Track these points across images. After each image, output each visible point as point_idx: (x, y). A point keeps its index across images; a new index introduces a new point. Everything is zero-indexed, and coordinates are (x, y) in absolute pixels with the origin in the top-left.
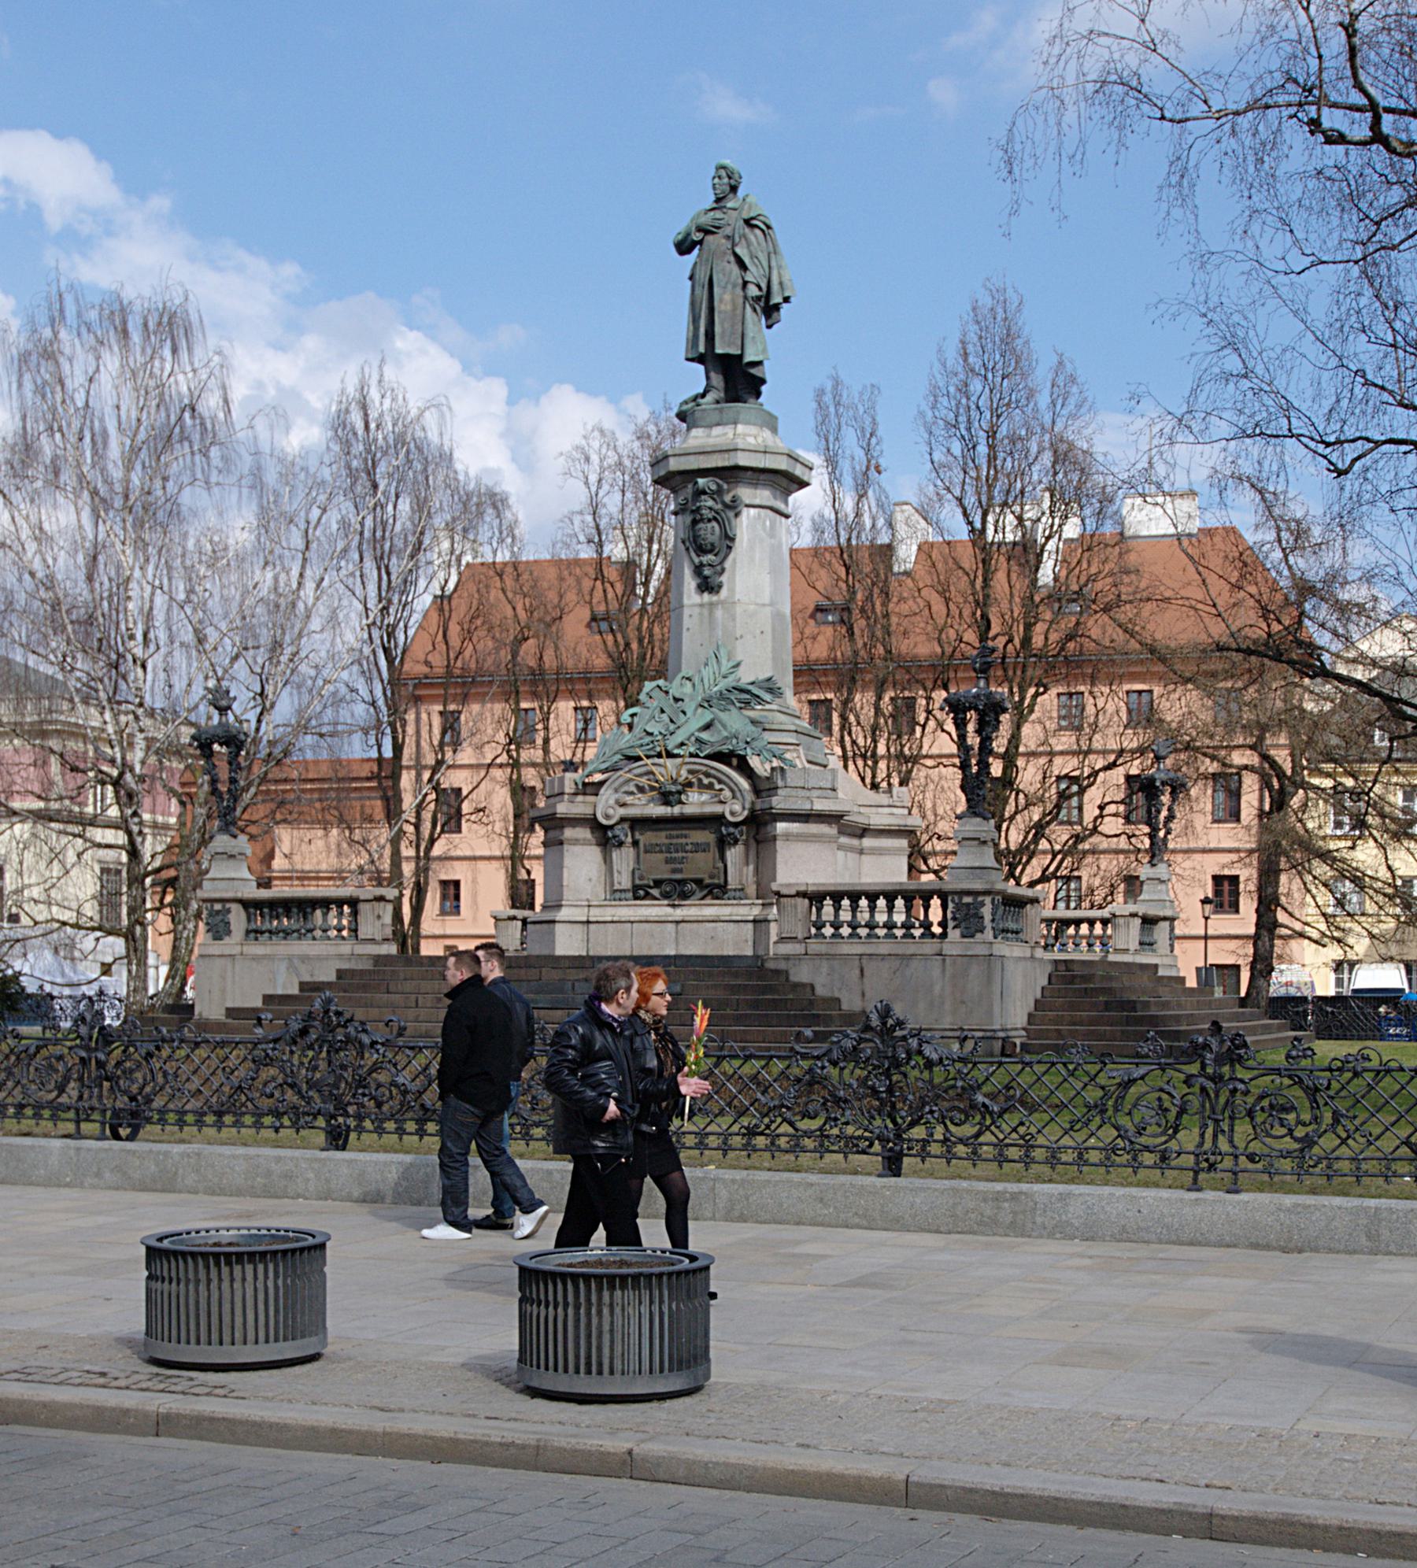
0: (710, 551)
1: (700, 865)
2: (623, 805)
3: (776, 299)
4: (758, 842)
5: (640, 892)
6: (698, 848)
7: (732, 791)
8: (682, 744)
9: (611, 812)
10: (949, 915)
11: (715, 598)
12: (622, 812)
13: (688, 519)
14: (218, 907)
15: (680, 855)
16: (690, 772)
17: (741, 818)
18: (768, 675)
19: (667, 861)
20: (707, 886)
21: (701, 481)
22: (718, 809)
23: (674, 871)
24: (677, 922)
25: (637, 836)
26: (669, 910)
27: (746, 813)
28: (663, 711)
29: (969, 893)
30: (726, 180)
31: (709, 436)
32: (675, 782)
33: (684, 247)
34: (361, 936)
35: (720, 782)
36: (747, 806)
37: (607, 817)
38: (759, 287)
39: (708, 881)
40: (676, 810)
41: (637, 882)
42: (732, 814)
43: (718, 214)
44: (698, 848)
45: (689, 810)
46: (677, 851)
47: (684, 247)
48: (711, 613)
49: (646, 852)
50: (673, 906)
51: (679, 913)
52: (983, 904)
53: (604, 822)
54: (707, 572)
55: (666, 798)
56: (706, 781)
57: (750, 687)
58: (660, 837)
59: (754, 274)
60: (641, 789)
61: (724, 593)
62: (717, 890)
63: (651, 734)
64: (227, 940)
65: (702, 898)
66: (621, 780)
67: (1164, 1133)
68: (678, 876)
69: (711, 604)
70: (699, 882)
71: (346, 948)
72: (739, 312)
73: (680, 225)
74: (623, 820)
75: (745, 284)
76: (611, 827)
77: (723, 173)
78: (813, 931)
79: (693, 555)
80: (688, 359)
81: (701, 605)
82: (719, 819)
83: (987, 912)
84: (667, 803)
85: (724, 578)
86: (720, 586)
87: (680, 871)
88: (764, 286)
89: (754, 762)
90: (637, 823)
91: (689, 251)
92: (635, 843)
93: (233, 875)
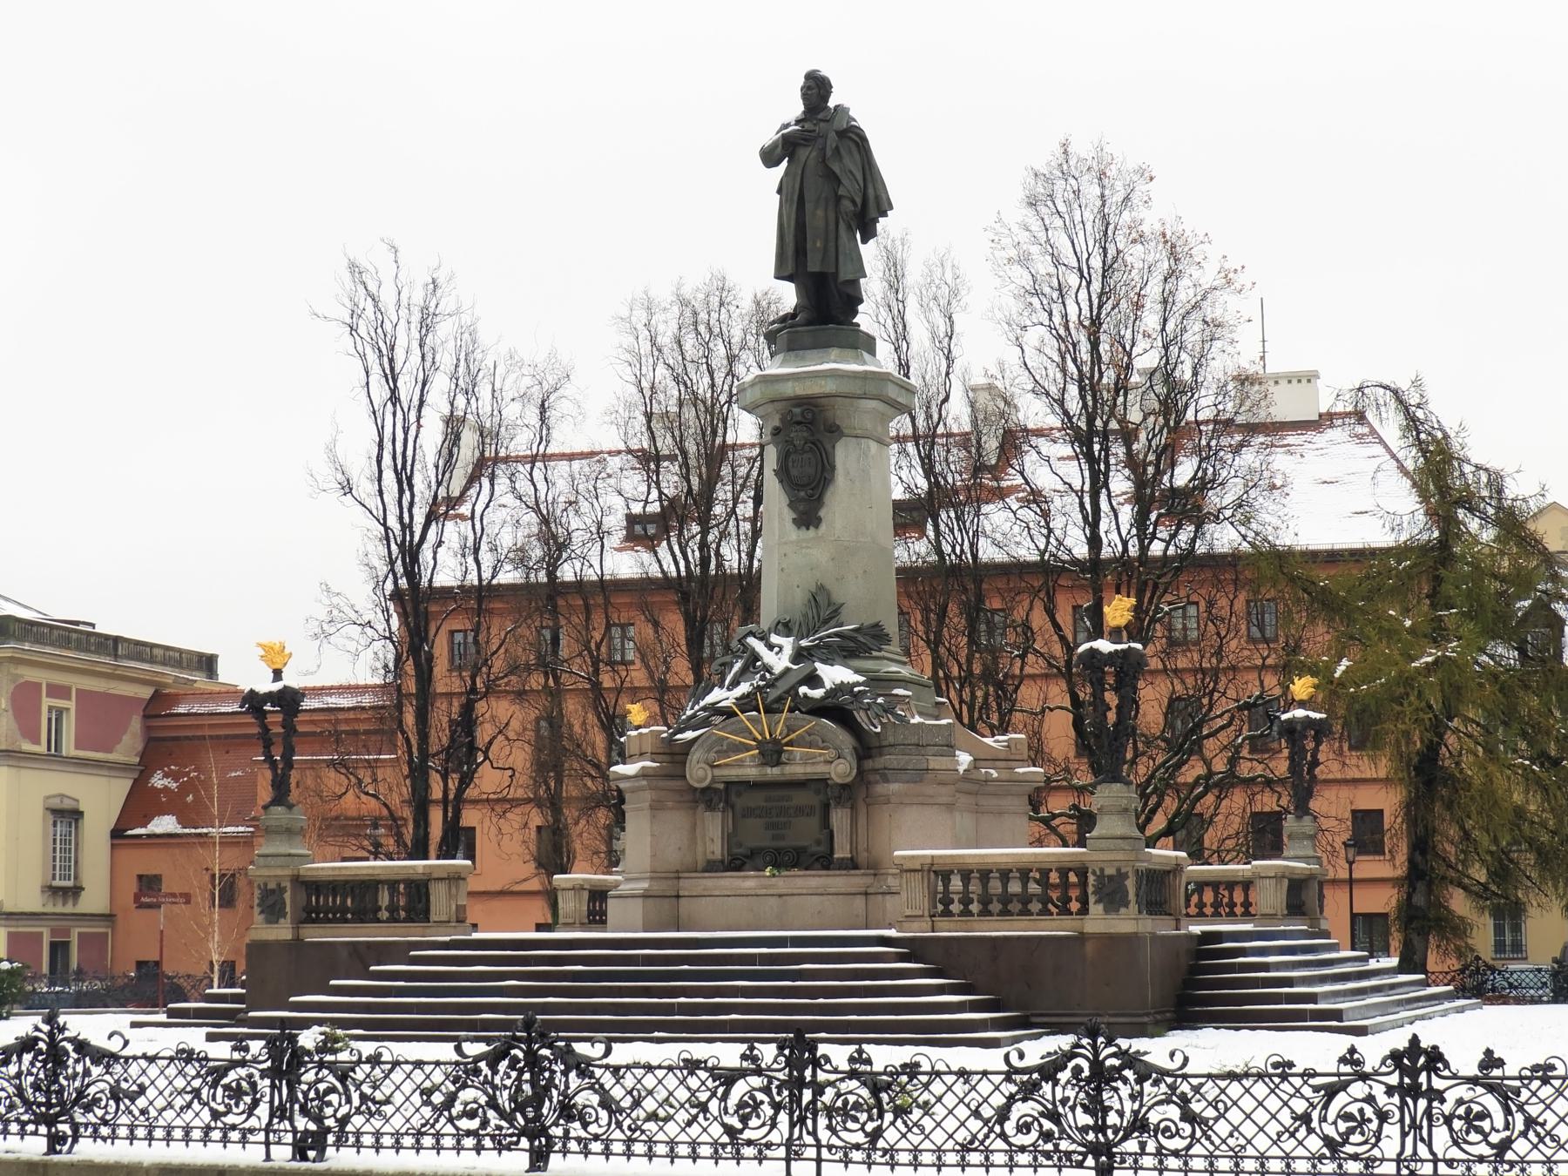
1: (804, 832)
3: (872, 213)
4: (868, 805)
5: (735, 862)
6: (800, 811)
8: (780, 699)
9: (701, 773)
10: (1090, 889)
11: (812, 532)
15: (782, 819)
16: (791, 730)
17: (849, 779)
18: (872, 621)
19: (769, 826)
22: (821, 769)
23: (774, 838)
33: (770, 157)
34: (433, 917)
38: (854, 202)
39: (815, 849)
41: (736, 851)
43: (808, 126)
44: (800, 811)
47: (770, 157)
52: (1126, 876)
56: (808, 738)
58: (756, 800)
59: (849, 187)
61: (823, 527)
62: (824, 861)
67: (1366, 1142)
68: (781, 844)
70: (800, 851)
72: (832, 227)
73: (769, 136)
74: (713, 780)
75: (838, 199)
77: (811, 83)
78: (940, 907)
80: (777, 277)
82: (822, 782)
83: (1130, 884)
86: (820, 520)
87: (782, 837)
88: (859, 201)
89: (860, 717)
90: (734, 787)
91: (777, 164)
92: (729, 805)
93: (293, 851)
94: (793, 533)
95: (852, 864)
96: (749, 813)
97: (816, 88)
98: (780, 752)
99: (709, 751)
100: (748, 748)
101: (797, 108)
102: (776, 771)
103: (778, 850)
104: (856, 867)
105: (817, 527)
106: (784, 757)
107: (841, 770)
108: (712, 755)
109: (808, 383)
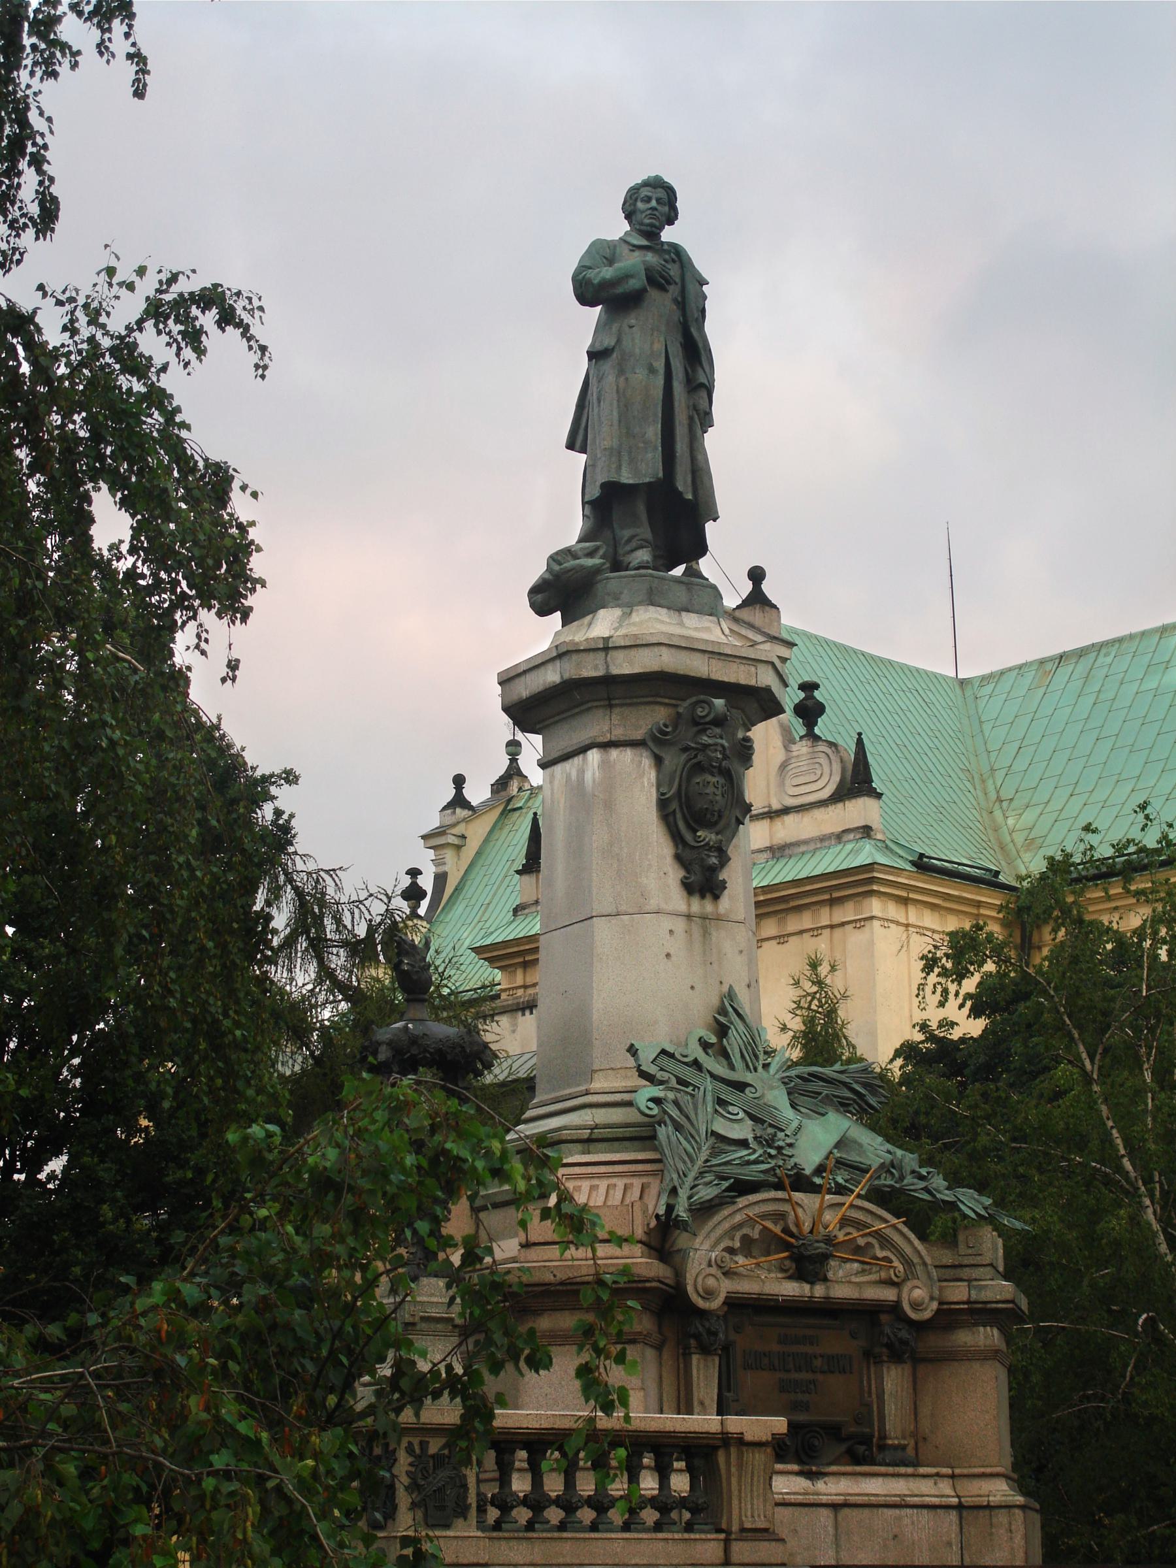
0: (710, 825)
6: (836, 1364)
8: (820, 1170)
9: (711, 1282)
11: (708, 906)
12: (726, 1286)
13: (674, 760)
16: (845, 1222)
17: (927, 1315)
20: (849, 1437)
21: (719, 702)
22: (889, 1294)
24: (835, 1507)
25: (733, 1336)
26: (802, 1483)
27: (935, 1305)
28: (721, 1102)
30: (666, 209)
31: (681, 624)
32: (829, 1240)
35: (885, 1242)
36: (936, 1293)
37: (709, 1294)
40: (819, 1291)
42: (916, 1306)
44: (836, 1364)
45: (841, 1292)
46: (799, 1369)
48: (706, 933)
49: (747, 1366)
50: (811, 1476)
51: (833, 1488)
53: (701, 1303)
55: (807, 1262)
56: (861, 1242)
57: (843, 1077)
62: (863, 1448)
63: (743, 1143)
66: (726, 1225)
69: (704, 918)
70: (834, 1431)
71: (709, 1549)
76: (702, 1313)
79: (681, 825)
81: (689, 917)
84: (800, 1275)
86: (723, 886)
97: (652, 205)
98: (825, 1257)
99: (713, 1248)
101: (617, 228)
102: (819, 1291)
105: (716, 897)
107: (919, 1297)
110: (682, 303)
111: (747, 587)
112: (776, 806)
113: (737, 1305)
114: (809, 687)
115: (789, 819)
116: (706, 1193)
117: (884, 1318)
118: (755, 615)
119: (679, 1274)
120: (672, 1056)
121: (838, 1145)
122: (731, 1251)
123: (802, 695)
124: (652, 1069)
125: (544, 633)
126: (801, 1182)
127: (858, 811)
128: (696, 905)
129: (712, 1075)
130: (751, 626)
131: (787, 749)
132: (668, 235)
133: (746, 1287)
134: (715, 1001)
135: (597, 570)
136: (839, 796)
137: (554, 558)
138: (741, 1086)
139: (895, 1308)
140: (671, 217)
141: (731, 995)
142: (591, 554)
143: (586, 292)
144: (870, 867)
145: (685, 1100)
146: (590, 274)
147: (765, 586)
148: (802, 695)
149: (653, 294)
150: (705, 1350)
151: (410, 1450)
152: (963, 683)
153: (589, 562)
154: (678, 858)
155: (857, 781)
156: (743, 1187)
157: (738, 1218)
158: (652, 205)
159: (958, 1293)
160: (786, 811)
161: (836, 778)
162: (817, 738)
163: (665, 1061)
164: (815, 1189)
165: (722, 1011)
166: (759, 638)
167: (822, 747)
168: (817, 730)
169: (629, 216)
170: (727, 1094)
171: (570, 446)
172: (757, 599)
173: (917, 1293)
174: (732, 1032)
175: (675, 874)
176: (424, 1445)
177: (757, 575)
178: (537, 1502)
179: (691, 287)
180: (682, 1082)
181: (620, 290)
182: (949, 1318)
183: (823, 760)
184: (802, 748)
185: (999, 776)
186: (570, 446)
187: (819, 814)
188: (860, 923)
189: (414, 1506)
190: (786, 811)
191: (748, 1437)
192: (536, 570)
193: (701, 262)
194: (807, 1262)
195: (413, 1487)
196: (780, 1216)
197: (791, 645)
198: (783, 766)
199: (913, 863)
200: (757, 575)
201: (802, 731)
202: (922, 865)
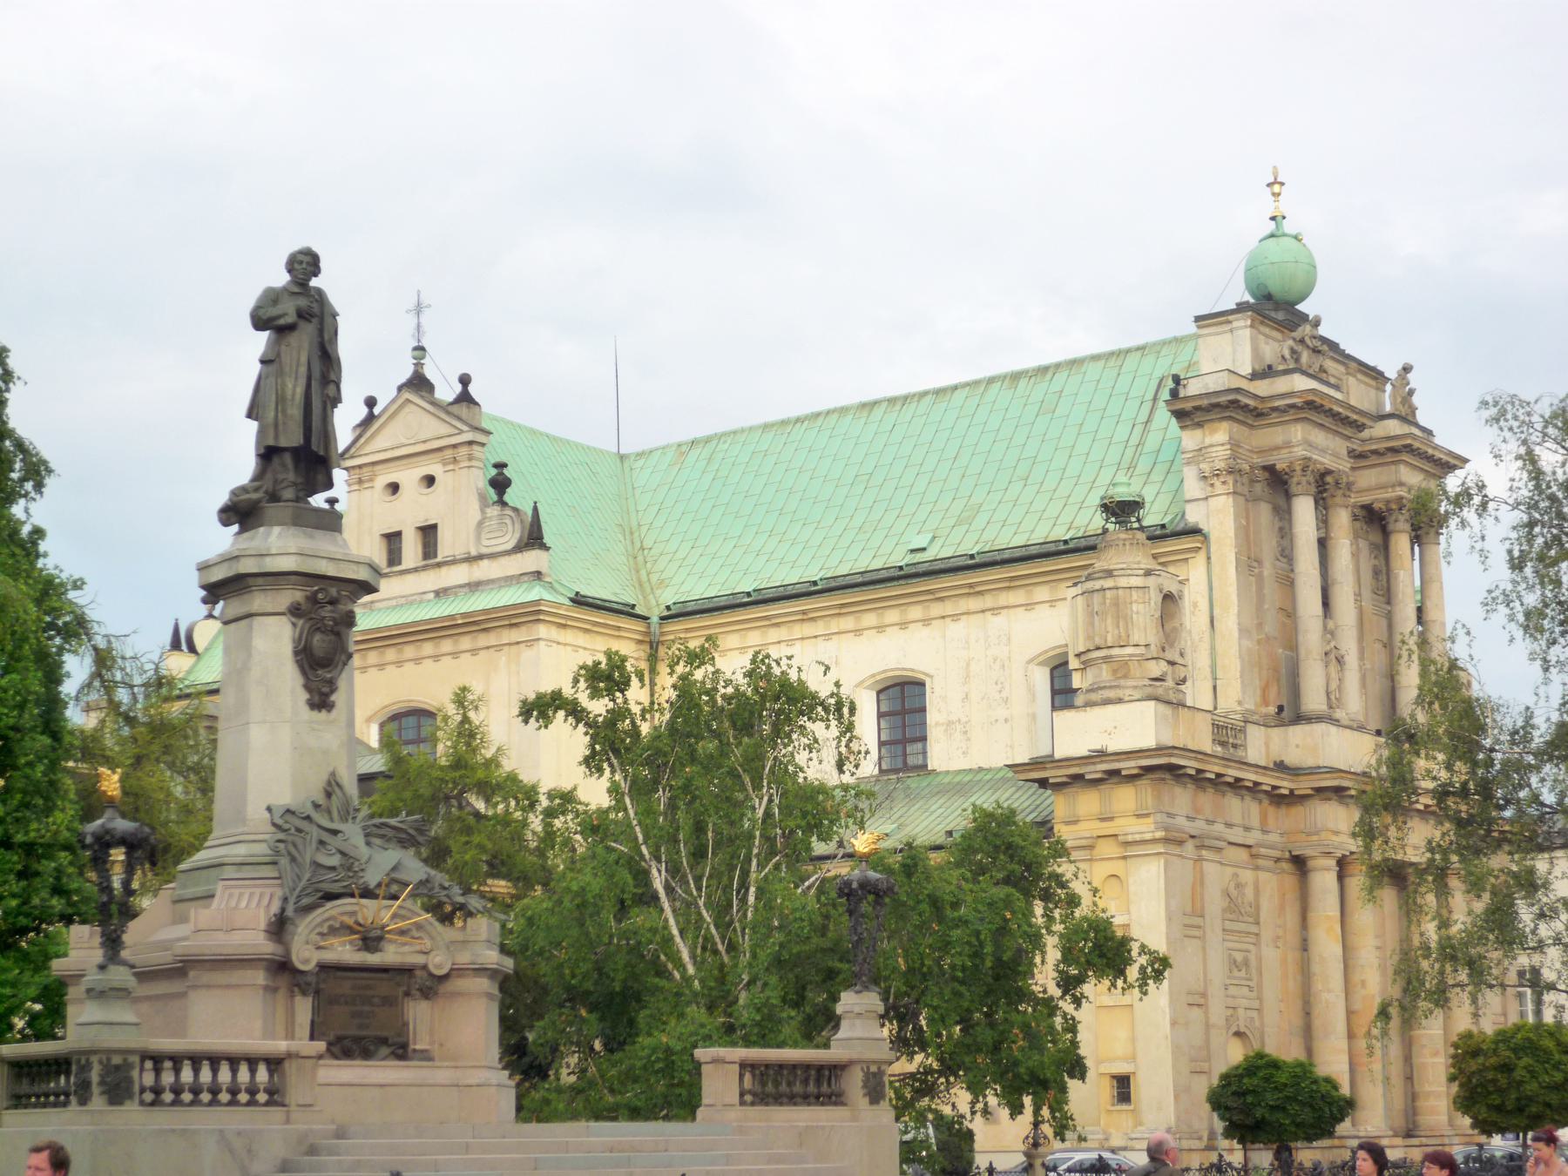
2: (319, 948)
7: (432, 938)
9: (307, 954)
11: (323, 715)
14: (117, 1060)
15: (366, 1008)
16: (394, 916)
19: (354, 1015)
22: (420, 960)
23: (360, 1027)
24: (382, 1086)
25: (322, 986)
28: (322, 843)
29: (874, 1062)
32: (383, 927)
37: (307, 961)
42: (439, 966)
54: (326, 690)
60: (333, 931)
62: (401, 1051)
63: (333, 868)
64: (128, 1102)
65: (384, 1059)
66: (319, 920)
68: (364, 1033)
70: (384, 1041)
71: (276, 1113)
76: (302, 972)
82: (406, 971)
85: (333, 698)
92: (317, 992)
94: (306, 713)
95: (425, 1056)
96: (333, 1001)
97: (305, 265)
100: (351, 931)
101: (281, 278)
103: (357, 1040)
104: (431, 1059)
106: (384, 944)
107: (439, 962)
108: (314, 937)
109: (342, 565)
110: (321, 331)
111: (458, 388)
112: (474, 553)
113: (324, 968)
114: (500, 466)
115: (485, 562)
116: (305, 901)
117: (418, 973)
118: (462, 410)
119: (288, 953)
120: (293, 813)
121: (394, 869)
122: (321, 934)
123: (494, 472)
124: (279, 822)
125: (224, 539)
126: (367, 893)
127: (532, 560)
128: (315, 715)
129: (319, 826)
130: (459, 419)
131: (483, 512)
132: (314, 282)
133: (329, 956)
134: (325, 777)
135: (259, 501)
136: (519, 548)
137: (234, 493)
138: (335, 832)
139: (424, 967)
140: (316, 271)
141: (333, 774)
142: (257, 490)
143: (259, 323)
144: (538, 602)
145: (299, 841)
146: (261, 312)
147: (472, 389)
148: (494, 472)
149: (302, 324)
150: (304, 993)
151: (100, 1062)
152: (622, 458)
153: (255, 496)
154: (307, 687)
155: (534, 538)
156: (330, 897)
157: (326, 915)
158: (305, 265)
159: (464, 958)
160: (480, 557)
161: (517, 535)
162: (504, 504)
163: (289, 817)
164: (375, 897)
165: (329, 783)
166: (465, 428)
167: (508, 512)
168: (506, 498)
169: (289, 271)
170: (326, 837)
171: (249, 416)
172: (465, 398)
173: (438, 960)
174: (334, 797)
175: (304, 696)
176: (109, 1059)
177: (465, 380)
178: (177, 1090)
179: (328, 319)
180: (299, 830)
181: (282, 322)
182: (456, 972)
183: (508, 521)
184: (494, 511)
185: (644, 529)
186: (249, 416)
187: (504, 560)
188: (530, 643)
189: (103, 1093)
190: (480, 557)
191: (304, 1054)
192: (223, 498)
193: (335, 299)
194: (371, 941)
195: (102, 1083)
196: (353, 913)
197: (489, 433)
198: (480, 524)
199: (572, 600)
200: (465, 380)
201: (495, 498)
202: (579, 601)
